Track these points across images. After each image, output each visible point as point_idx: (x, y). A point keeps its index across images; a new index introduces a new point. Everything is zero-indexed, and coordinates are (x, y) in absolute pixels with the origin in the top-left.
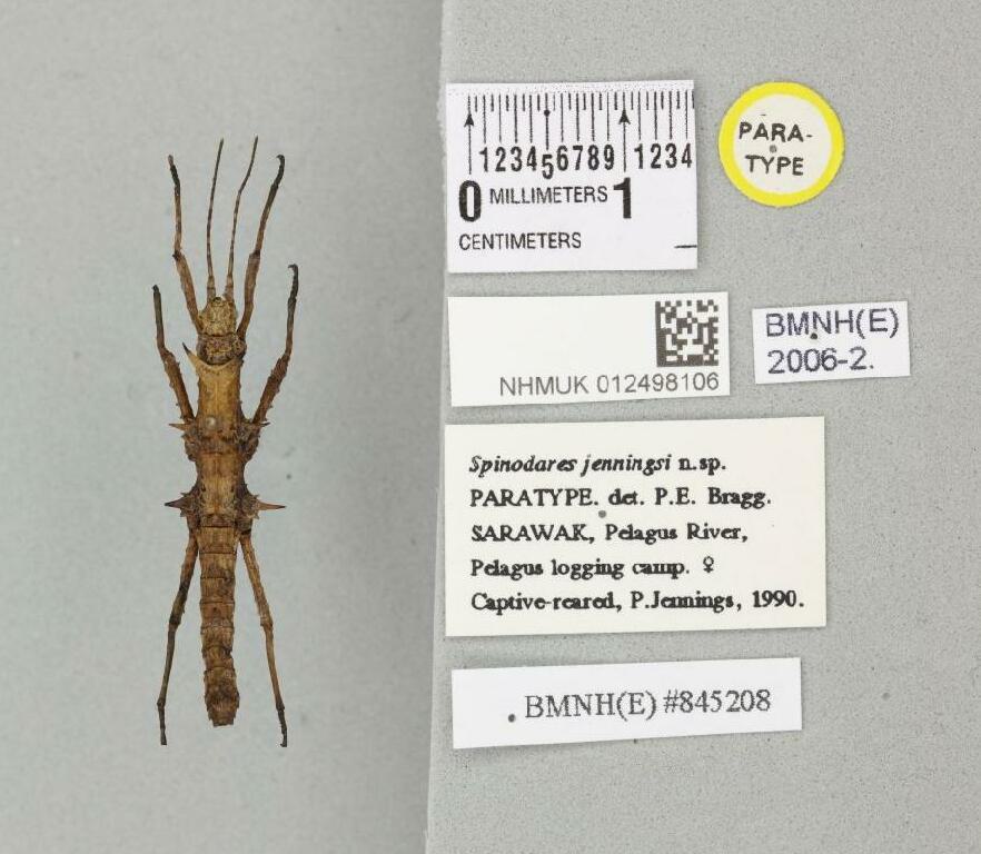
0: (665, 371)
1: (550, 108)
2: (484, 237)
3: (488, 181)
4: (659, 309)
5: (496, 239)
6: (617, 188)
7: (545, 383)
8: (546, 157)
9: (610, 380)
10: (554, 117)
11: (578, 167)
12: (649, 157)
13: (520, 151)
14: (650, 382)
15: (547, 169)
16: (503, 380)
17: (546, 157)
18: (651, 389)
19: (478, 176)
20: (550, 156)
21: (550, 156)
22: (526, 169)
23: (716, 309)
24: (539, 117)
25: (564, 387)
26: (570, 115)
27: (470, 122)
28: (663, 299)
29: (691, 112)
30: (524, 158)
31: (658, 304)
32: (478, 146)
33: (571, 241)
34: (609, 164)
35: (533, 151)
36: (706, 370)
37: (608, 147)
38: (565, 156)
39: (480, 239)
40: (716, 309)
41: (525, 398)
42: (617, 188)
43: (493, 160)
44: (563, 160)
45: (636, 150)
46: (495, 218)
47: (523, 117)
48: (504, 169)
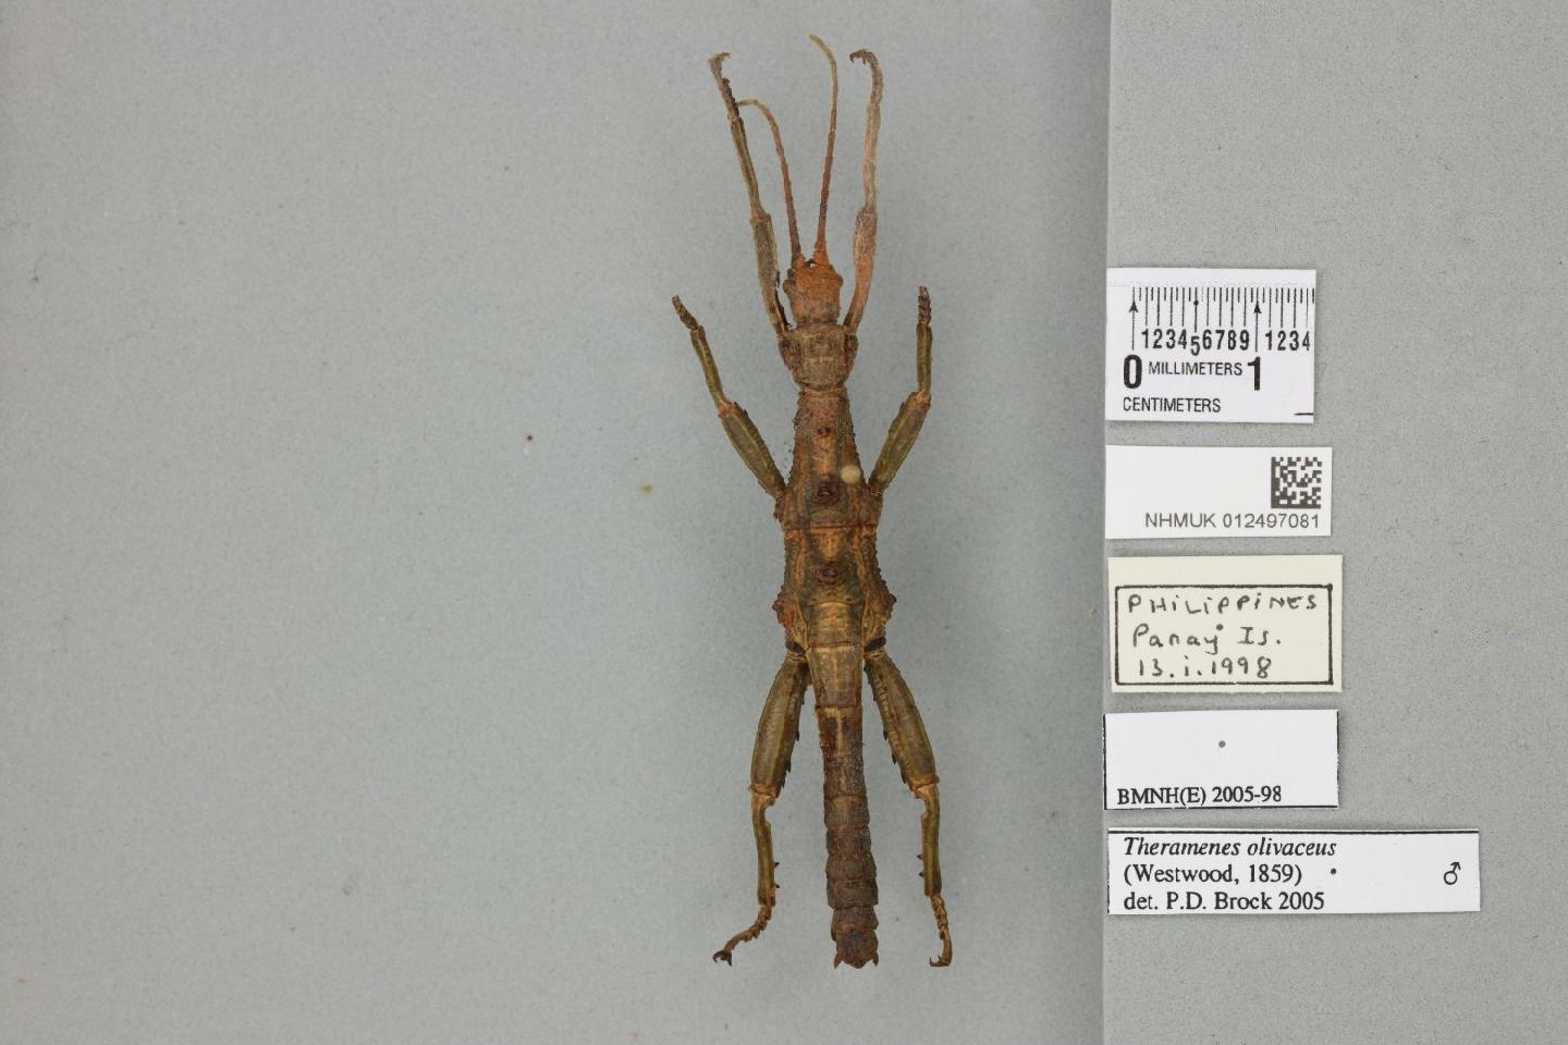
0: (1277, 511)
1: (1199, 299)
2: (1144, 400)
3: (1149, 356)
4: (1274, 463)
6: (1250, 364)
7: (1180, 518)
8: (1193, 338)
9: (1233, 519)
10: (1202, 306)
11: (1219, 347)
12: (1276, 340)
13: (1174, 333)
14: (1265, 520)
15: (1195, 347)
16: (1148, 515)
17: (1193, 338)
18: (1265, 525)
19: (1140, 351)
20: (1198, 338)
21: (1198, 338)
22: (1178, 347)
23: (1320, 464)
24: (1190, 306)
25: (1196, 521)
26: (1214, 306)
27: (1134, 308)
28: (1278, 453)
29: (1312, 307)
30: (1177, 338)
31: (1273, 459)
32: (1141, 327)
33: (1212, 406)
34: (1244, 345)
35: (1184, 333)
36: (1311, 512)
37: (1244, 332)
38: (1209, 338)
39: (1140, 401)
40: (1320, 464)
41: (1166, 531)
42: (1250, 364)
44: (1207, 341)
45: (1267, 335)
46: (1152, 385)
47: (1177, 305)
48: (1160, 347)
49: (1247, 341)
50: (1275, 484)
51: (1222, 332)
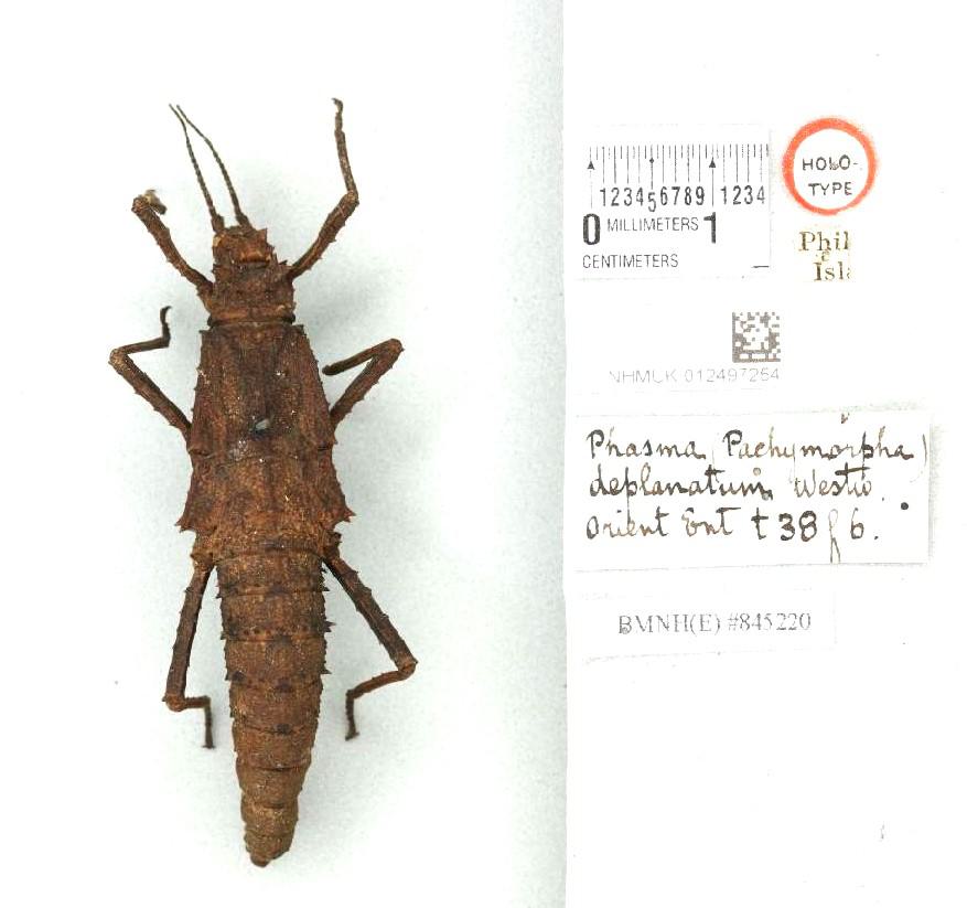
3: (606, 213)
4: (735, 318)
5: (611, 258)
6: (706, 219)
22: (636, 204)
26: (669, 162)
33: (669, 260)
34: (700, 200)
35: (641, 190)
40: (778, 318)
42: (706, 219)
43: (610, 196)
46: (610, 242)
48: (617, 204)
49: (702, 196)
50: (737, 337)
51: (677, 188)
